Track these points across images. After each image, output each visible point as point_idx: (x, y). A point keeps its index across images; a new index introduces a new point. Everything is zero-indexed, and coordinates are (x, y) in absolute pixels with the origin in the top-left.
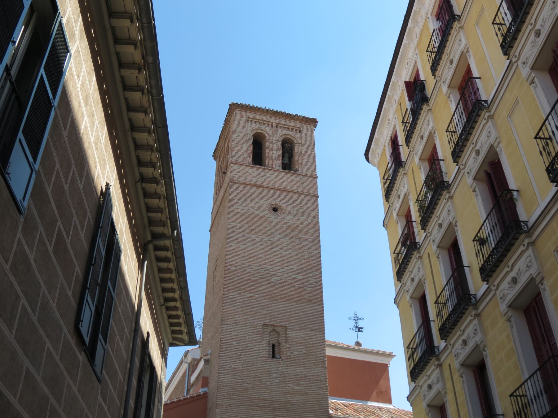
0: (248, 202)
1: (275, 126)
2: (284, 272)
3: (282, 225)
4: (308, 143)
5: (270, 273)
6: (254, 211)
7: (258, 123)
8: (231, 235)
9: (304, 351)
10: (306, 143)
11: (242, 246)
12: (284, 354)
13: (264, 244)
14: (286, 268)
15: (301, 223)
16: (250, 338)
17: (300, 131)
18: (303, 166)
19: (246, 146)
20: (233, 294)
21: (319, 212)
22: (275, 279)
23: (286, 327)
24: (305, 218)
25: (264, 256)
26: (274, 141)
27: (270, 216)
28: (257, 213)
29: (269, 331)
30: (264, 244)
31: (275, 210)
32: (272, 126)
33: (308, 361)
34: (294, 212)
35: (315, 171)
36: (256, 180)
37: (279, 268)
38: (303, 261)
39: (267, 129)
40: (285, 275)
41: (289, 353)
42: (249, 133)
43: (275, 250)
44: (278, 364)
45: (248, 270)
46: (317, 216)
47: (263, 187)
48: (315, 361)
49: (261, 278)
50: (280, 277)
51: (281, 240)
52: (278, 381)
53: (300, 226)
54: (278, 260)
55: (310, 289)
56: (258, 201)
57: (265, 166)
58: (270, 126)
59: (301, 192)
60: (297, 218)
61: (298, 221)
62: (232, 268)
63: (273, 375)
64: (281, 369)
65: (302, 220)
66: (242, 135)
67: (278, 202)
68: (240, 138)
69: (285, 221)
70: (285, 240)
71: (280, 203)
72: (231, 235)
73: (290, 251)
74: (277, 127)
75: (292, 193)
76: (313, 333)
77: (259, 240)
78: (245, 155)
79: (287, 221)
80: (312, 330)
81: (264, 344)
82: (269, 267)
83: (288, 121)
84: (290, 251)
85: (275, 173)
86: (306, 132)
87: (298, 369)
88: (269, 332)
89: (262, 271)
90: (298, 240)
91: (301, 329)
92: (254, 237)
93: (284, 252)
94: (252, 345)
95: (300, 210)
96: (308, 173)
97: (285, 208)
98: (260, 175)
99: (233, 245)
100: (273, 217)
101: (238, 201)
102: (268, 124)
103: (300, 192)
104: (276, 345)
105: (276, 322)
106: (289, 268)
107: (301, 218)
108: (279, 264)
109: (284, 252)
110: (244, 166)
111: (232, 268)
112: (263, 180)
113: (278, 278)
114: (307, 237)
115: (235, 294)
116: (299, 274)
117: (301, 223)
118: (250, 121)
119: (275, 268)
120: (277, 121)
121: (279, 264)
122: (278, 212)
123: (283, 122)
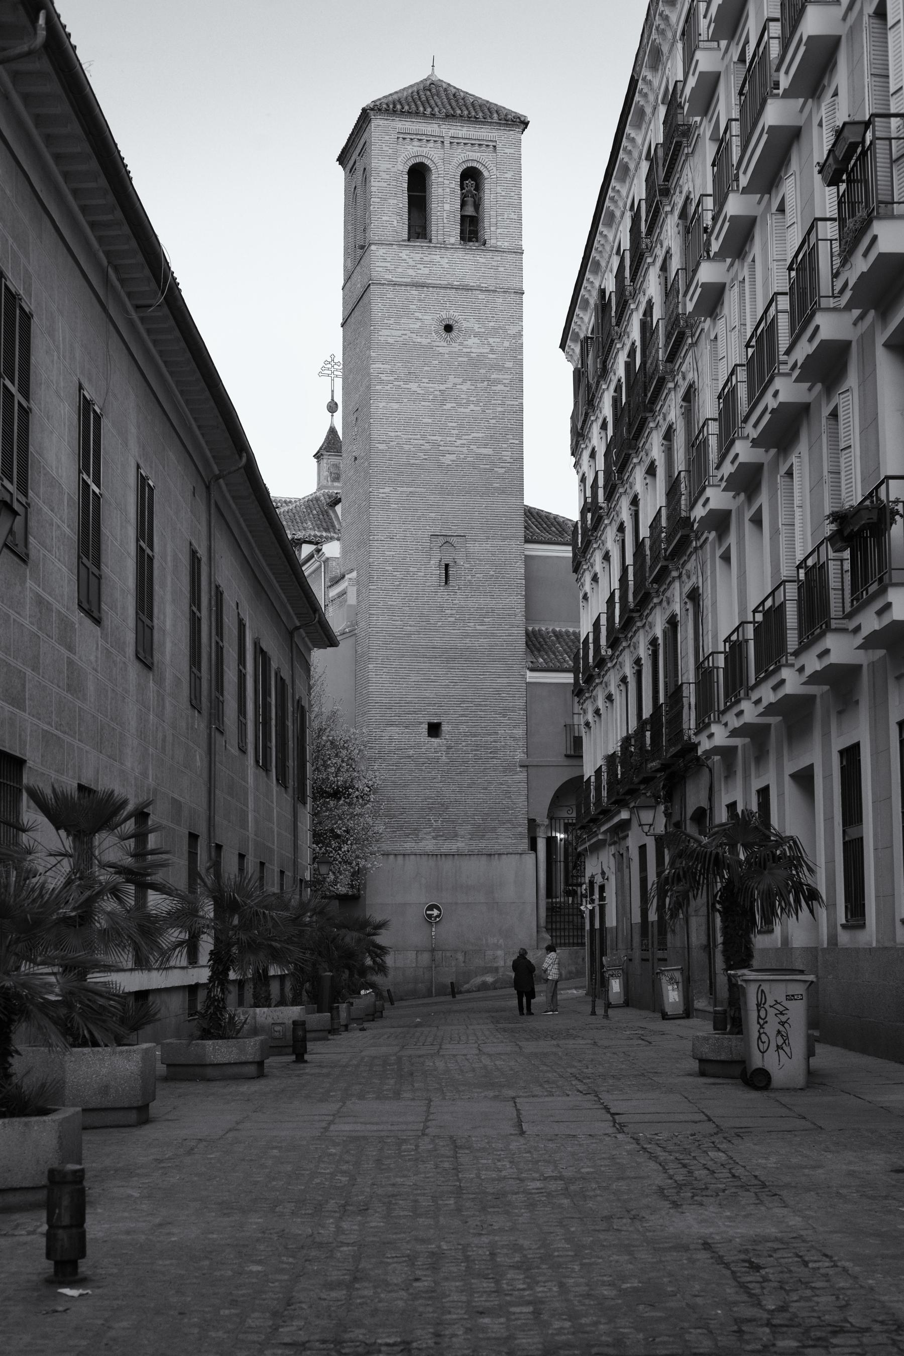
1: (447, 144)
2: (463, 445)
3: (460, 359)
4: (509, 175)
5: (441, 448)
6: (414, 335)
8: (378, 387)
9: (492, 573)
10: (506, 175)
11: (396, 406)
13: (431, 397)
14: (466, 437)
18: (499, 231)
19: (395, 202)
21: (524, 324)
22: (448, 459)
25: (430, 421)
26: (446, 182)
28: (419, 340)
31: (448, 328)
34: (480, 330)
35: (521, 239)
36: (414, 274)
37: (454, 439)
38: (494, 421)
39: (432, 153)
40: (465, 450)
42: (401, 168)
45: (406, 447)
46: (520, 335)
51: (458, 387)
53: (490, 356)
54: (454, 424)
57: (430, 241)
59: (493, 288)
62: (382, 447)
65: (493, 344)
67: (453, 314)
68: (385, 185)
69: (465, 350)
70: (464, 387)
72: (378, 387)
73: (472, 407)
75: (478, 292)
77: (422, 392)
78: (395, 223)
79: (468, 350)
80: (504, 539)
82: (439, 438)
83: (472, 129)
84: (472, 407)
85: (448, 253)
86: (507, 151)
89: (427, 447)
90: (486, 383)
92: (413, 386)
93: (462, 410)
94: (415, 570)
95: (492, 324)
96: (506, 244)
97: (465, 324)
98: (421, 262)
99: (381, 405)
100: (445, 344)
101: (386, 321)
103: (491, 288)
104: (451, 564)
105: (450, 529)
106: (470, 437)
107: (491, 340)
108: (456, 432)
110: (394, 247)
111: (382, 447)
112: (427, 271)
113: (453, 457)
114: (501, 377)
115: (387, 490)
116: (486, 446)
117: (492, 351)
119: (448, 439)
120: (452, 132)
121: (456, 432)
122: (454, 334)
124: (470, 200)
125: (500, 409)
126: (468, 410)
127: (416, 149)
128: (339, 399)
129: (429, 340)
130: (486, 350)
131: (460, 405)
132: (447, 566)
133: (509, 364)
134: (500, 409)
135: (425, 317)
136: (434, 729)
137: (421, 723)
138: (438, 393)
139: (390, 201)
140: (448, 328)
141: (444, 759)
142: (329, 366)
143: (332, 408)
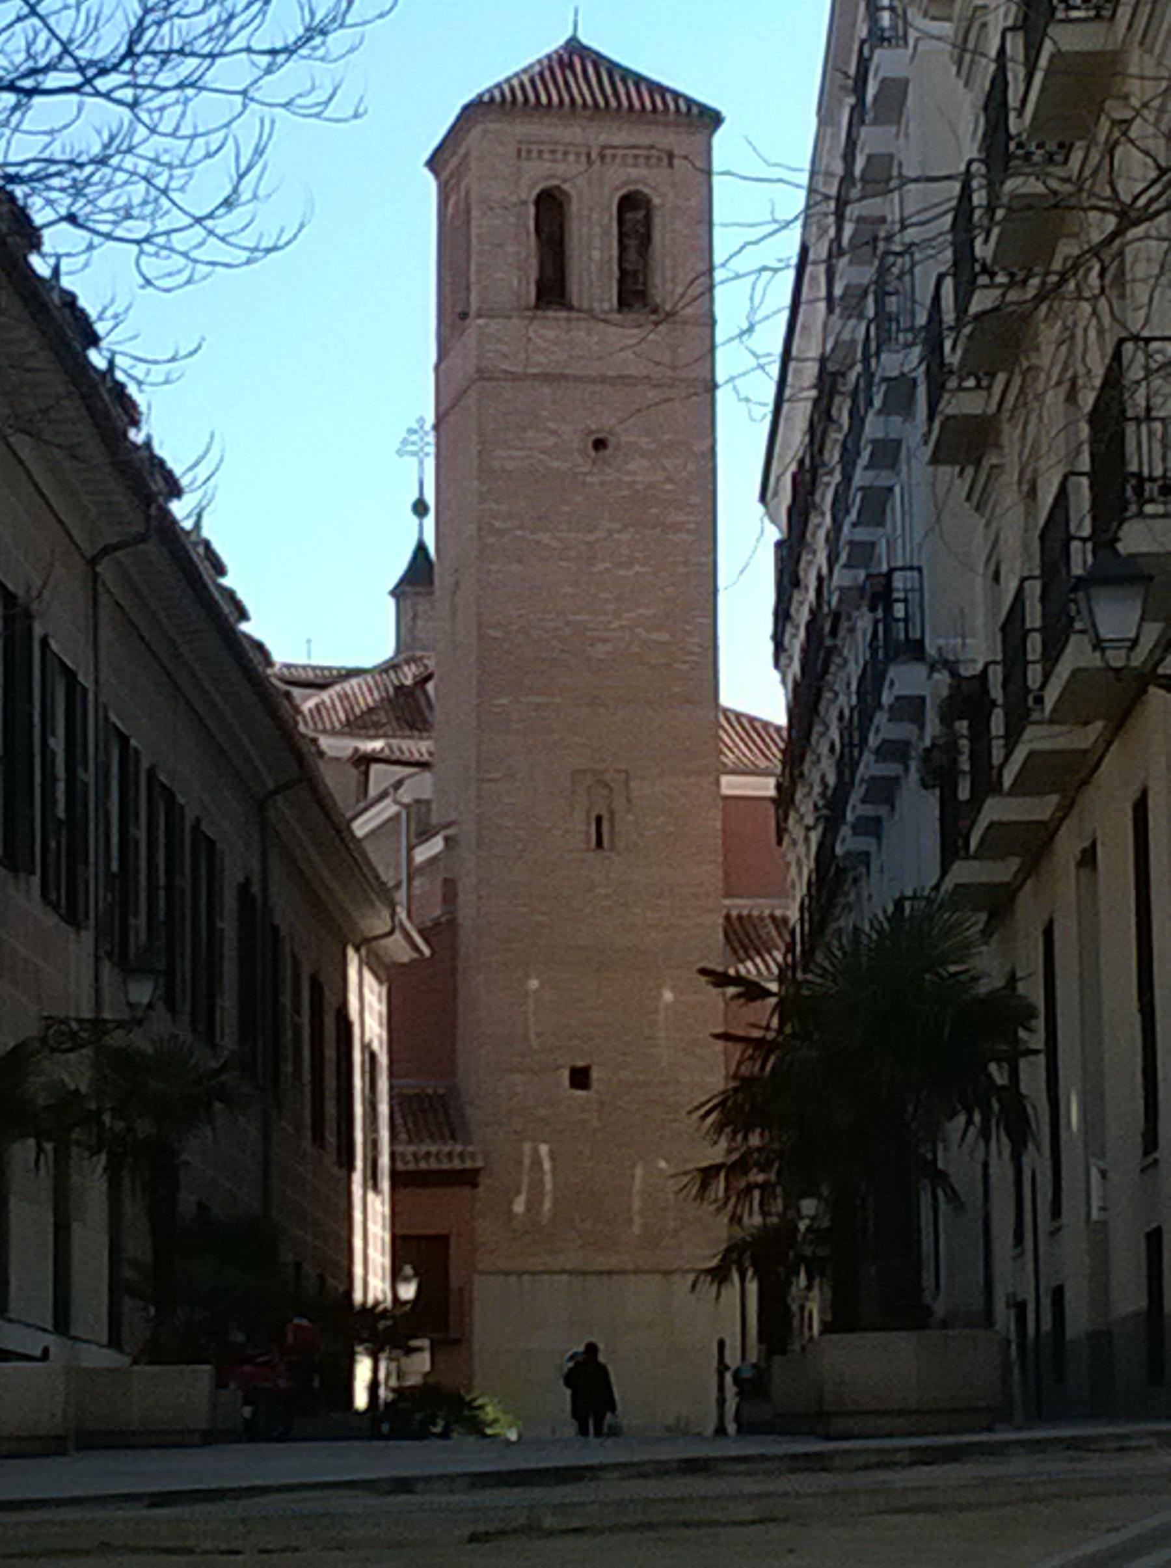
7: (546, 156)
11: (515, 567)
13: (573, 554)
22: (600, 651)
30: (573, 554)
32: (588, 155)
37: (609, 618)
43: (601, 567)
46: (712, 452)
47: (564, 377)
52: (608, 903)
55: (686, 667)
69: (627, 479)
70: (625, 537)
73: (637, 568)
74: (602, 157)
78: (515, 283)
82: (586, 618)
84: (637, 568)
89: (568, 631)
90: (658, 530)
92: (545, 538)
93: (622, 572)
95: (668, 437)
99: (494, 567)
102: (578, 155)
109: (622, 572)
113: (609, 647)
115: (504, 701)
117: (669, 480)
118: (524, 154)
120: (603, 138)
123: (620, 135)
124: (632, 243)
125: (682, 570)
126: (631, 573)
128: (430, 499)
129: (569, 465)
130: (659, 476)
131: (620, 565)
132: (599, 820)
133: (694, 499)
134: (682, 570)
136: (580, 1078)
137: (559, 1067)
138: (583, 547)
140: (600, 444)
141: (596, 1124)
142: (414, 438)
143: (420, 508)
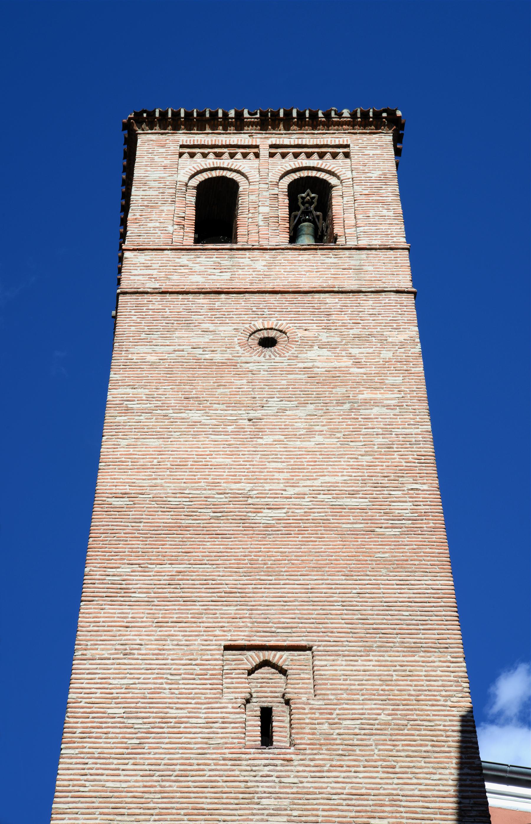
0: (177, 334)
1: (264, 152)
2: (301, 496)
5: (250, 501)
7: (211, 156)
12: (307, 731)
14: (309, 483)
15: (357, 363)
16: (177, 692)
17: (347, 155)
20: (118, 570)
23: (310, 649)
24: (371, 350)
25: (228, 461)
27: (249, 359)
29: (250, 667)
30: (230, 429)
32: (257, 155)
33: (400, 748)
34: (330, 340)
37: (281, 486)
41: (326, 726)
44: (282, 765)
48: (429, 748)
49: (217, 518)
50: (284, 511)
54: (279, 465)
56: (212, 327)
58: (251, 156)
60: (344, 353)
61: (345, 359)
62: (117, 502)
63: (264, 801)
64: (296, 780)
65: (358, 356)
66: (161, 185)
68: (156, 193)
70: (301, 413)
71: (283, 325)
76: (416, 658)
79: (310, 365)
81: (230, 706)
82: (248, 487)
84: (319, 439)
86: (367, 152)
87: (361, 775)
88: (251, 672)
90: (347, 406)
91: (369, 650)
92: (195, 416)
99: (124, 443)
100: (262, 359)
101: (143, 336)
106: (317, 483)
107: (355, 351)
108: (282, 476)
111: (117, 502)
112: (227, 276)
114: (379, 396)
116: (352, 494)
117: (357, 363)
127: (211, 161)
135: (221, 328)
139: (161, 208)
